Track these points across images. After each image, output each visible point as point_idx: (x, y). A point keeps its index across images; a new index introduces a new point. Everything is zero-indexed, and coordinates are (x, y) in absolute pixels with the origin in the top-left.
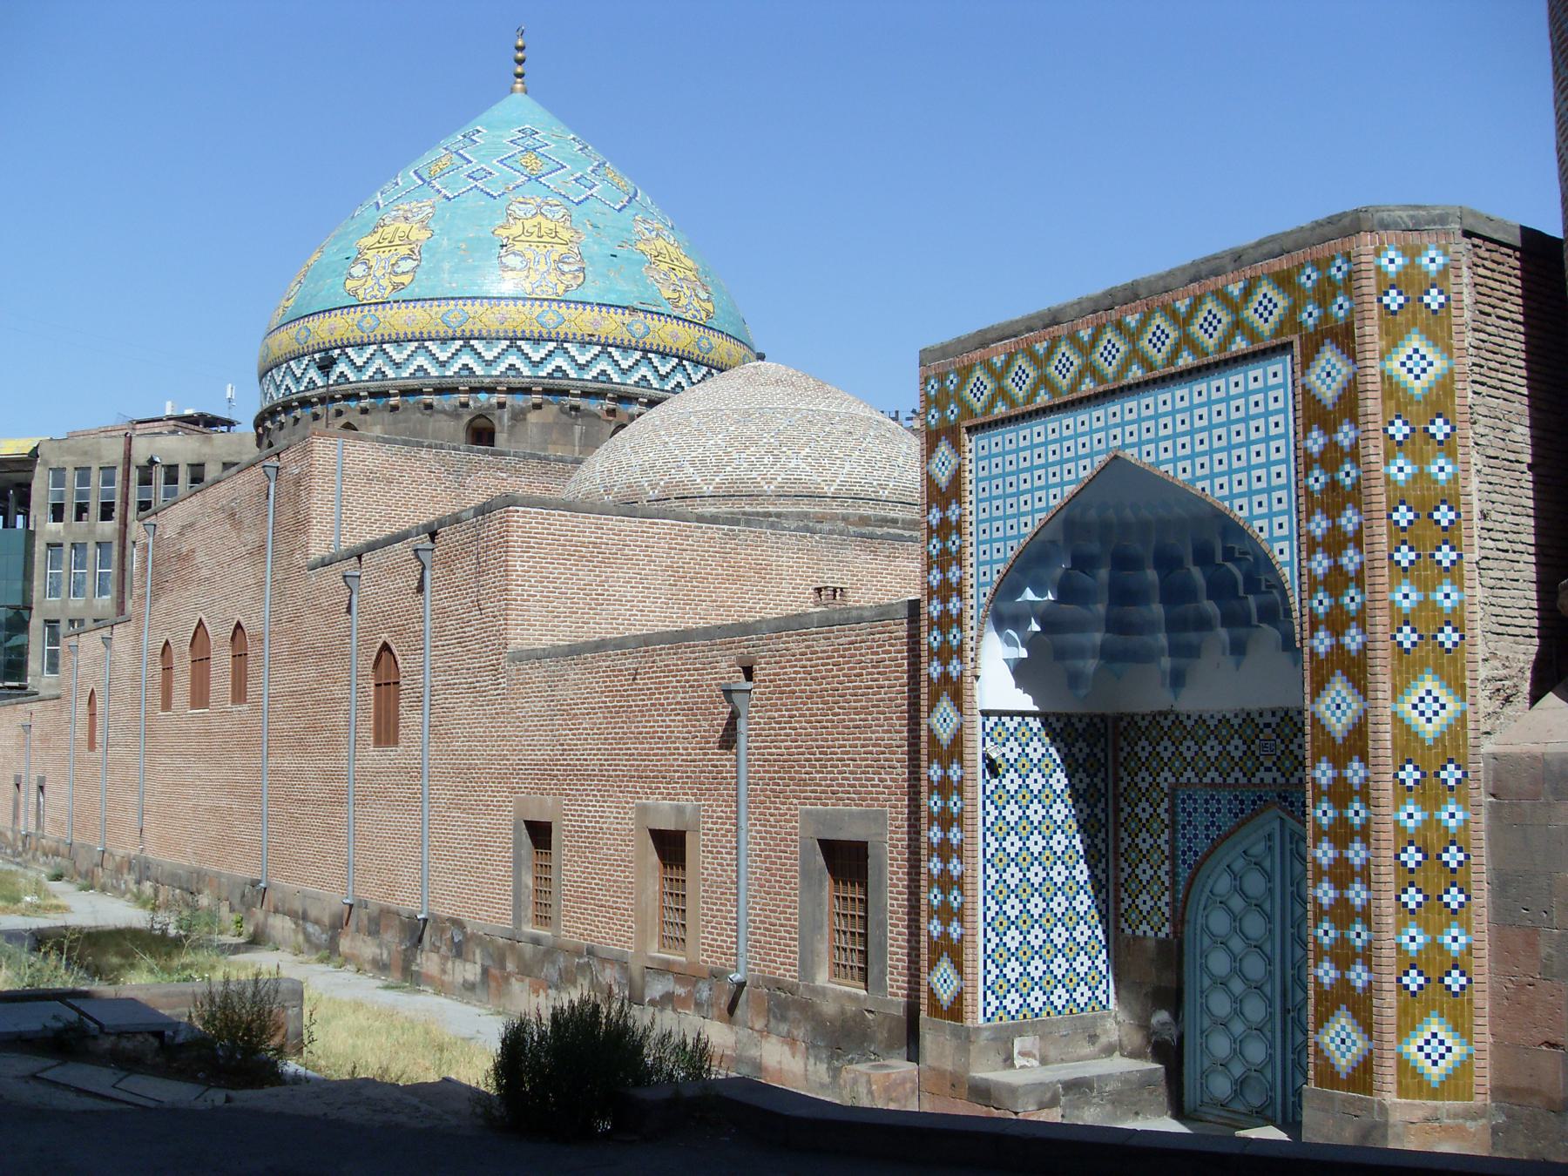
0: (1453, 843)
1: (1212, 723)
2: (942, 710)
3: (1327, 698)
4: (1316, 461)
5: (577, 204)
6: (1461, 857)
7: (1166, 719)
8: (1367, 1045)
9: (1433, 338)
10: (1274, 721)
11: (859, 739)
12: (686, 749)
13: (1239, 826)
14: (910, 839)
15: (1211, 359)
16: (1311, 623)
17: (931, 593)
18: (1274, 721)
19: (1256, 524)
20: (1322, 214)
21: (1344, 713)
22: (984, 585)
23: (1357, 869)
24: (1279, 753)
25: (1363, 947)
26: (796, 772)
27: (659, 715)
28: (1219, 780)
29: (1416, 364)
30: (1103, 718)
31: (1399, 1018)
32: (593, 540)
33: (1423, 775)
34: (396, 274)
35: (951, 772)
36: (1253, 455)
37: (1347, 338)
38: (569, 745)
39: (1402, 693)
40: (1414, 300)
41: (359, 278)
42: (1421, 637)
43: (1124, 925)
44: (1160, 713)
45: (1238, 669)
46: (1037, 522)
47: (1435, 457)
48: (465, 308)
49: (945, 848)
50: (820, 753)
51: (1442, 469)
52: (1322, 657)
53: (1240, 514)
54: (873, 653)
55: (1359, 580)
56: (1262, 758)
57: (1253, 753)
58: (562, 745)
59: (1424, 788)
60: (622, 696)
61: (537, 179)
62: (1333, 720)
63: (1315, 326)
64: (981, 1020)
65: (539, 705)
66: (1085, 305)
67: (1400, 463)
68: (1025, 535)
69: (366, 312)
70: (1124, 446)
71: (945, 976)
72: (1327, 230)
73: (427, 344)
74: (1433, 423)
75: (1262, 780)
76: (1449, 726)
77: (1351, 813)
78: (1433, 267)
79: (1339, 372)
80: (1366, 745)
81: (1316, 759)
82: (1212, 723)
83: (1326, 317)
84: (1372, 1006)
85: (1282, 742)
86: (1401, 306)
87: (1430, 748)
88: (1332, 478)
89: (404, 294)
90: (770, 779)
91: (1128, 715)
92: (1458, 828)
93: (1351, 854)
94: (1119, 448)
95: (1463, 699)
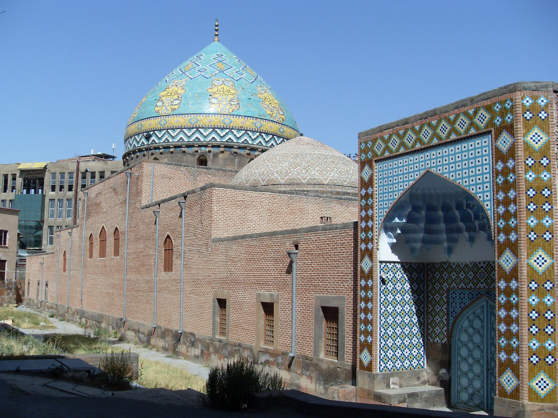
0: (549, 310)
1: (462, 266)
2: (365, 261)
3: (504, 257)
4: (500, 173)
5: (237, 81)
6: (552, 315)
7: (445, 264)
8: (517, 382)
9: (542, 129)
10: (484, 266)
11: (336, 271)
12: (274, 274)
13: (472, 303)
14: (354, 307)
15: (462, 136)
16: (498, 230)
17: (362, 219)
18: (484, 266)
19: (478, 195)
20: (502, 85)
21: (509, 263)
22: (381, 216)
23: (514, 319)
24: (486, 277)
25: (516, 347)
26: (313, 282)
27: (265, 262)
28: (464, 287)
29: (536, 138)
30: (423, 264)
31: (529, 374)
32: (242, 199)
33: (538, 285)
34: (173, 105)
35: (368, 283)
36: (477, 171)
37: (511, 129)
38: (233, 272)
39: (531, 256)
40: (536, 115)
41: (160, 107)
42: (537, 236)
43: (430, 338)
44: (443, 262)
45: (471, 247)
46: (400, 194)
47: (543, 171)
48: (197, 117)
49: (366, 310)
50: (322, 276)
51: (545, 176)
52: (502, 243)
53: (473, 192)
54: (341, 240)
55: (515, 215)
56: (480, 279)
57: (477, 277)
58: (230, 272)
59: (538, 290)
60: (252, 255)
61: (222, 72)
62: (506, 265)
63: (500, 124)
64: (378, 371)
65: (222, 258)
66: (417, 117)
67: (530, 174)
69: (162, 119)
70: (431, 167)
71: (366, 355)
72: (504, 90)
73: (183, 130)
74: (542, 159)
75: (480, 287)
76: (548, 268)
77: (512, 299)
78: (542, 104)
79: (508, 141)
80: (518, 274)
81: (499, 279)
82: (462, 266)
83: (503, 122)
85: (487, 273)
86: (531, 118)
87: (541, 276)
88: (506, 179)
89: (176, 112)
90: (304, 285)
91: (432, 263)
92: (551, 305)
93: (512, 314)
95: (553, 258)
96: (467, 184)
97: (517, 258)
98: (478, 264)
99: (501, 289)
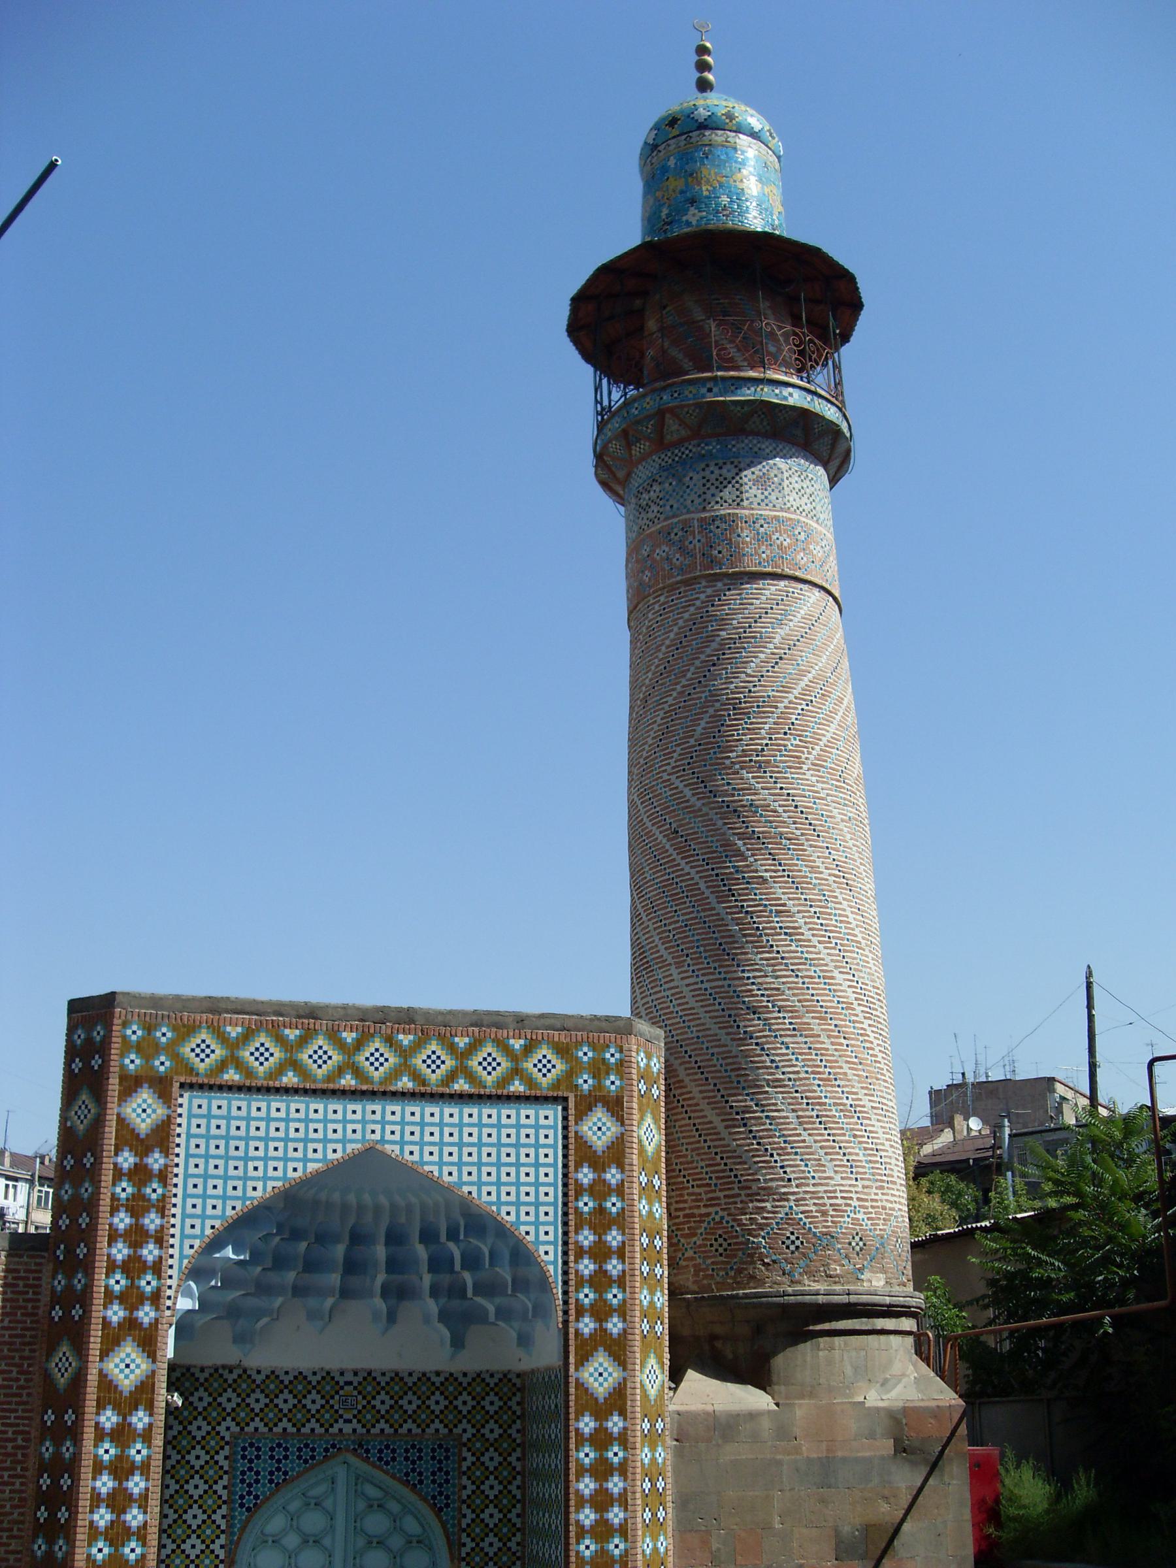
2: (123, 1355)
7: (231, 1372)
13: (306, 1470)
16: (577, 1310)
21: (606, 1380)
24: (360, 1407)
44: (224, 1367)
46: (269, 1189)
53: (507, 1218)
55: (621, 1282)
56: (341, 1412)
57: (332, 1407)
66: (349, 1012)
68: (252, 1198)
70: (383, 1141)
72: (604, 1024)
75: (341, 1430)
80: (625, 1404)
81: (579, 1414)
83: (599, 1086)
85: (364, 1398)
88: (600, 1205)
94: (377, 1142)
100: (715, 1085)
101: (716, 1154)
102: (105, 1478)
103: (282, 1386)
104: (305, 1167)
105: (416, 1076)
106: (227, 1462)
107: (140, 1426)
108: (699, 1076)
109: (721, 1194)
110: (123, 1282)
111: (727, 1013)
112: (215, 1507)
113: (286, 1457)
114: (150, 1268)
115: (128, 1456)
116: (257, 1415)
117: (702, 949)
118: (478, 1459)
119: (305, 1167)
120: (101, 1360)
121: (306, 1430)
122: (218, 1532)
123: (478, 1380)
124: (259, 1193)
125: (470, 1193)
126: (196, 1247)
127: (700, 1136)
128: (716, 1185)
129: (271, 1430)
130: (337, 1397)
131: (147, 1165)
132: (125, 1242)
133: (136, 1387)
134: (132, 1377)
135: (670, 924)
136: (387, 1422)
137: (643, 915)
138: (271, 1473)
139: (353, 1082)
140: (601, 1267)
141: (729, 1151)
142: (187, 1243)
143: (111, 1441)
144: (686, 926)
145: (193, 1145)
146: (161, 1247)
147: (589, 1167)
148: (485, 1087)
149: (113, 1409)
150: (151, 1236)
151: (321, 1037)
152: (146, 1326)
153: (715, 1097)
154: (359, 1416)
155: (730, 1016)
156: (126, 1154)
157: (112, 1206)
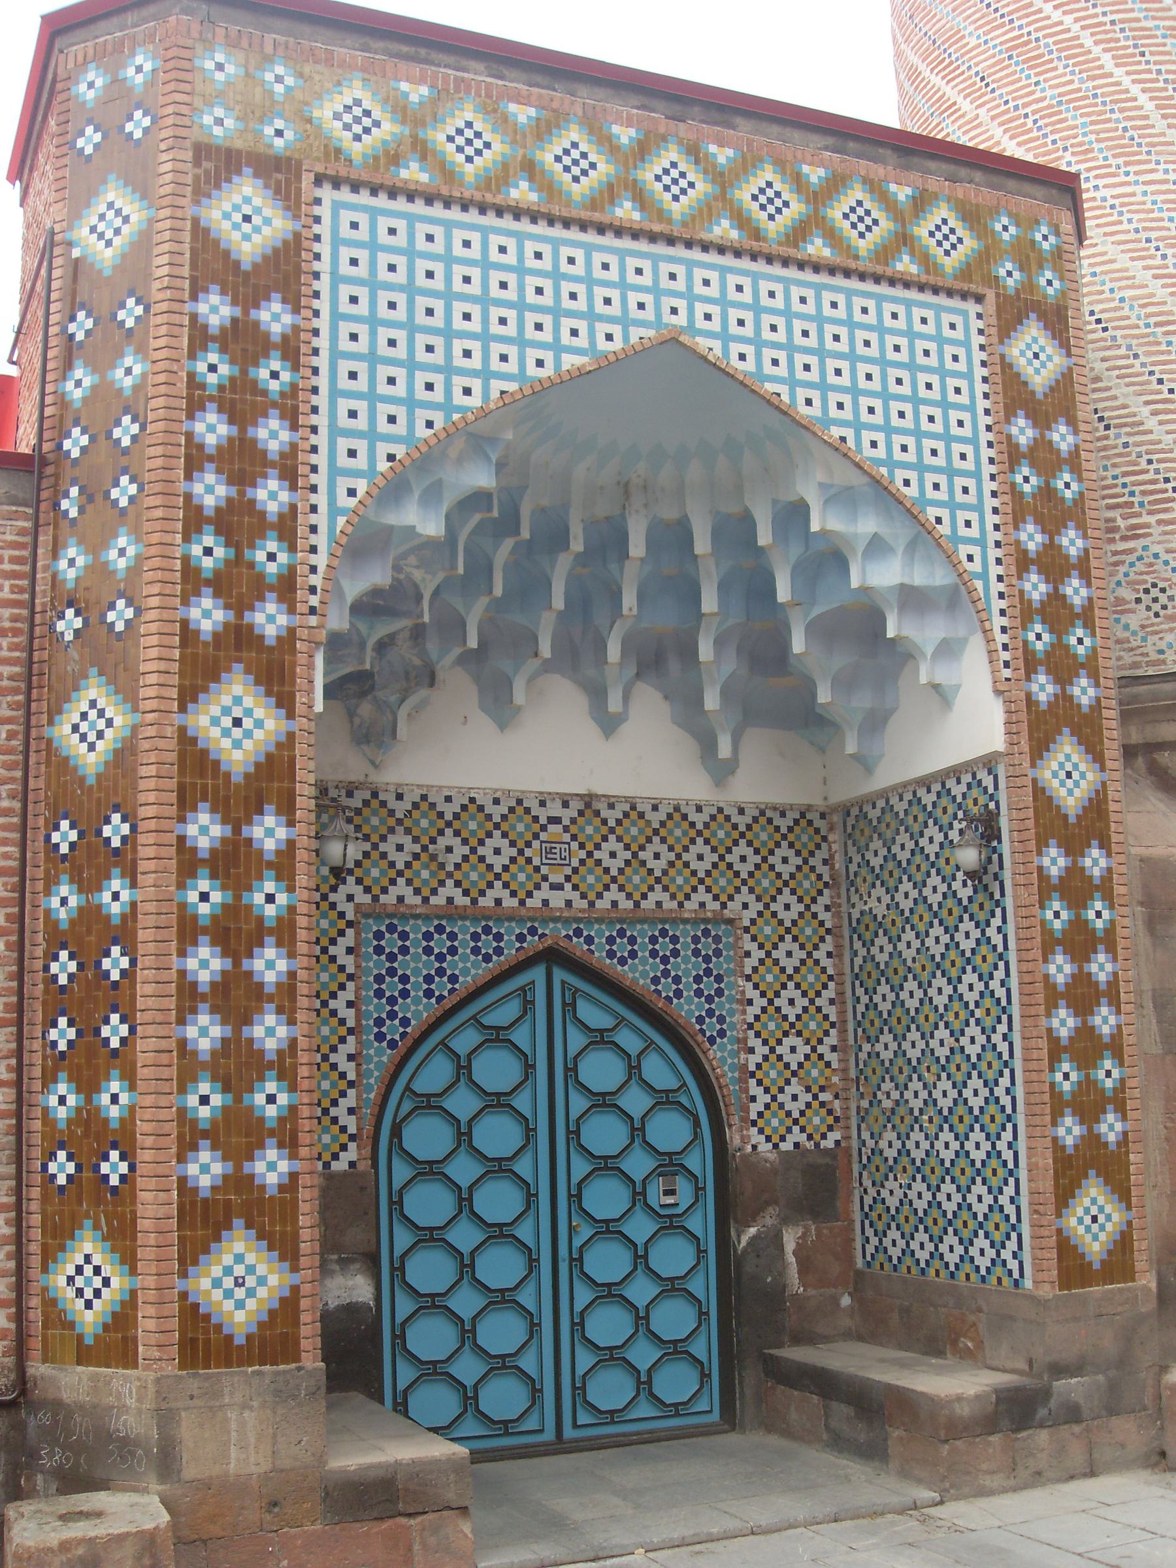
2: (226, 700)
7: (350, 794)
8: (1126, 1216)
10: (567, 815)
24: (575, 863)
25: (1114, 1089)
28: (462, 901)
46: (494, 395)
52: (1044, 707)
53: (905, 490)
56: (544, 870)
57: (529, 861)
75: (545, 902)
77: (1091, 915)
80: (1108, 827)
84: (1128, 1164)
85: (582, 846)
88: (1047, 483)
93: (1094, 968)
94: (681, 330)
96: (881, 452)
97: (1103, 769)
98: (533, 804)
99: (1049, 877)
100: (1129, 348)
101: (1139, 456)
102: (204, 952)
103: (441, 824)
104: (558, 361)
105: (741, 220)
106: (351, 958)
107: (270, 845)
108: (1101, 334)
109: (1152, 519)
110: (220, 552)
111: (1143, 235)
112: (334, 1040)
113: (453, 951)
114: (272, 526)
115: (249, 907)
116: (400, 874)
117: (1093, 137)
118: (768, 954)
119: (558, 361)
120: (183, 709)
121: (486, 902)
122: (343, 1085)
123: (762, 820)
124: (475, 401)
125: (843, 439)
126: (361, 493)
127: (1107, 427)
128: (1141, 504)
129: (426, 900)
130: (536, 844)
131: (256, 324)
132: (219, 471)
133: (257, 765)
134: (248, 744)
135: (1025, 105)
136: (621, 888)
137: (965, 105)
138: (429, 979)
139: (636, 216)
140: (1056, 589)
141: (1162, 451)
142: (343, 484)
143: (213, 876)
144: (1060, 103)
145: (344, 298)
146: (293, 487)
147: (1027, 417)
148: (856, 257)
149: (213, 810)
150: (273, 465)
151: (574, 127)
152: (270, 642)
153: (1132, 366)
154: (575, 879)
155: (1148, 240)
156: (215, 299)
157: (190, 398)
